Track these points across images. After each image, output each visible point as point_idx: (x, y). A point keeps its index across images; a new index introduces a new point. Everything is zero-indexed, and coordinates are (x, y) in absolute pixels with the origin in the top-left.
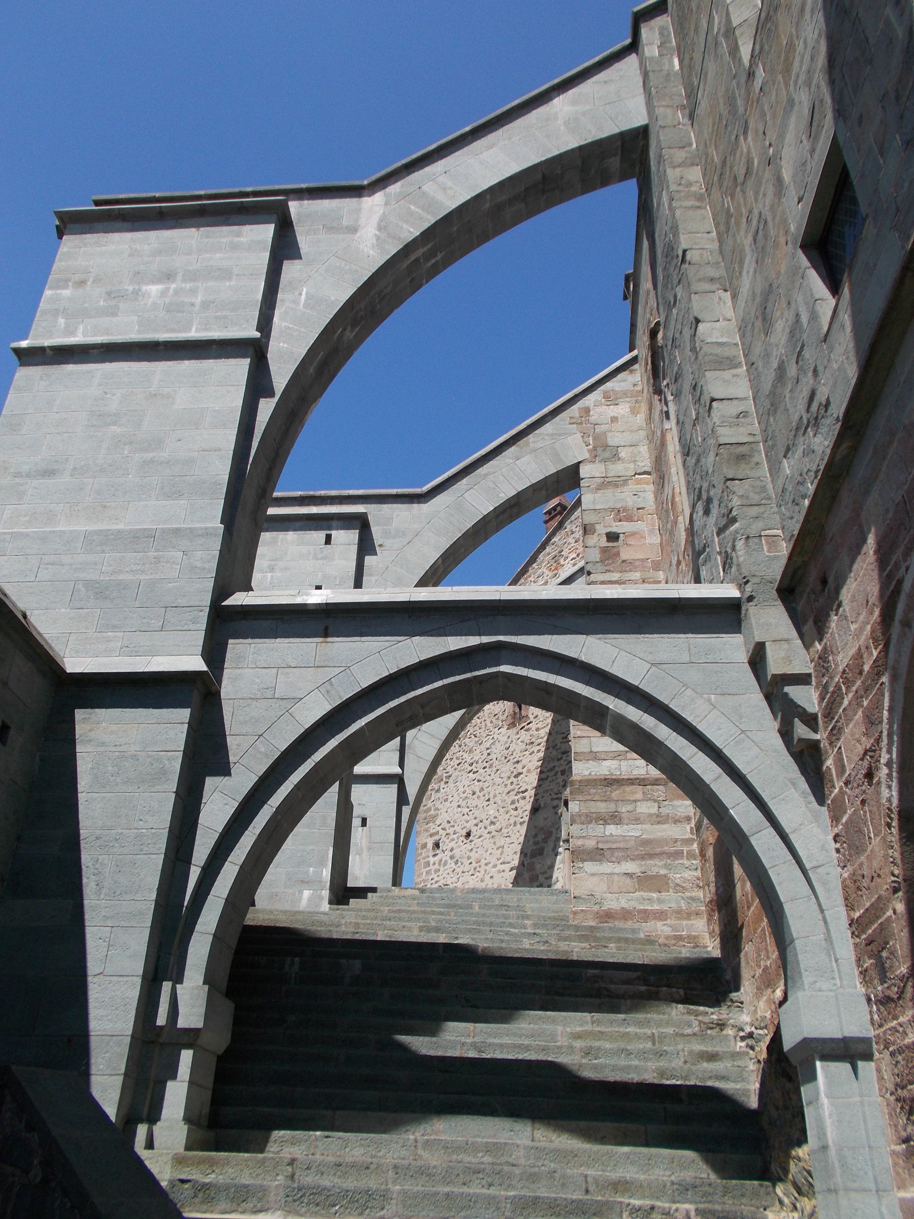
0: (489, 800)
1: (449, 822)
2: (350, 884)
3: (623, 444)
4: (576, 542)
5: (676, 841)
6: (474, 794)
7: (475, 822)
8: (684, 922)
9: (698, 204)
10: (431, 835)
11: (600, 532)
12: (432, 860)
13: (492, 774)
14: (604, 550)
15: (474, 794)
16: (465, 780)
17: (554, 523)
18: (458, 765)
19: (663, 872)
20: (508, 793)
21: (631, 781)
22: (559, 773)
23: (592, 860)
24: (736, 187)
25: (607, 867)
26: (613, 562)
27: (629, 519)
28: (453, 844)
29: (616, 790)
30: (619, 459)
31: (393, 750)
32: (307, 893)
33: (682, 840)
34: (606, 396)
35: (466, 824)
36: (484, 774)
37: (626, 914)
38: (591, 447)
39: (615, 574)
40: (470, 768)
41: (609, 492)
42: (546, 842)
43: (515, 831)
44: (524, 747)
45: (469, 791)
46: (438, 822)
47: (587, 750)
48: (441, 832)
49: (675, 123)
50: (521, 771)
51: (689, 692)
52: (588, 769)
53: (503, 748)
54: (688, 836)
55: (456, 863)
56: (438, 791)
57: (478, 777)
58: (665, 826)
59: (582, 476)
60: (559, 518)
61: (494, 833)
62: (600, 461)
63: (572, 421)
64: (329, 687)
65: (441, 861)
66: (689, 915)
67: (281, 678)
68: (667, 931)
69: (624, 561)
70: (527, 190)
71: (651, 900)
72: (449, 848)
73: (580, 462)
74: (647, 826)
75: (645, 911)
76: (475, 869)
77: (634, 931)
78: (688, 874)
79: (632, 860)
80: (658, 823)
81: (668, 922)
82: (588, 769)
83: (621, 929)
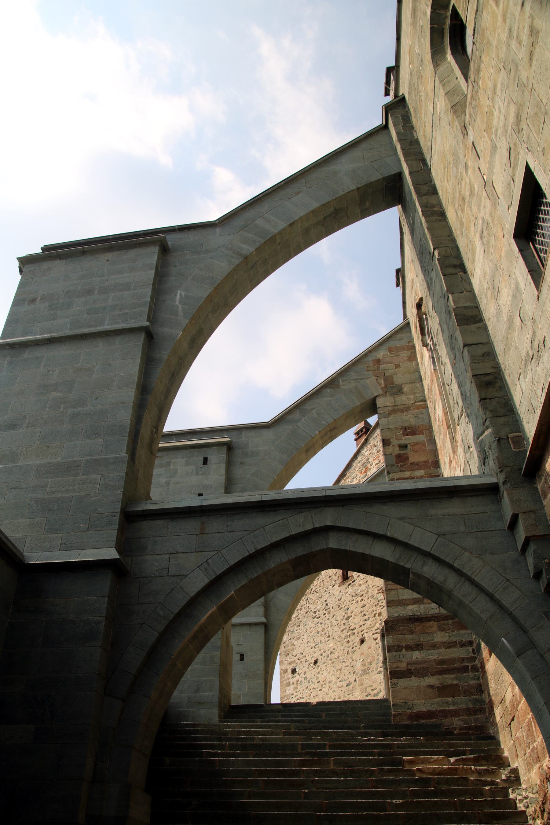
0: (329, 637)
2: (233, 703)
3: (405, 382)
4: (378, 452)
5: (463, 660)
6: (318, 633)
7: (320, 652)
8: (472, 717)
9: (440, 218)
10: (290, 664)
11: (394, 444)
12: (291, 681)
13: (330, 618)
14: (399, 456)
15: (318, 633)
16: (311, 624)
17: (363, 440)
19: (455, 682)
20: (342, 631)
21: (429, 619)
22: (377, 615)
24: (465, 204)
25: (414, 682)
26: (405, 464)
27: (414, 433)
28: (306, 669)
29: (418, 626)
30: (403, 393)
33: (468, 658)
34: (390, 350)
35: (314, 655)
36: (324, 619)
37: (430, 714)
38: (383, 385)
39: (406, 473)
40: (314, 615)
41: (397, 416)
42: (371, 664)
43: (349, 658)
44: (351, 598)
48: (297, 661)
49: (419, 169)
50: (350, 615)
52: (397, 612)
54: (471, 655)
55: (309, 682)
58: (455, 649)
59: (378, 406)
61: (334, 660)
62: (390, 395)
64: (206, 566)
65: (298, 681)
66: (475, 712)
68: (460, 724)
70: (325, 218)
72: (303, 672)
73: (375, 397)
76: (322, 686)
77: (438, 726)
78: (473, 682)
79: (432, 675)
80: (450, 648)
81: (461, 717)
82: (397, 612)
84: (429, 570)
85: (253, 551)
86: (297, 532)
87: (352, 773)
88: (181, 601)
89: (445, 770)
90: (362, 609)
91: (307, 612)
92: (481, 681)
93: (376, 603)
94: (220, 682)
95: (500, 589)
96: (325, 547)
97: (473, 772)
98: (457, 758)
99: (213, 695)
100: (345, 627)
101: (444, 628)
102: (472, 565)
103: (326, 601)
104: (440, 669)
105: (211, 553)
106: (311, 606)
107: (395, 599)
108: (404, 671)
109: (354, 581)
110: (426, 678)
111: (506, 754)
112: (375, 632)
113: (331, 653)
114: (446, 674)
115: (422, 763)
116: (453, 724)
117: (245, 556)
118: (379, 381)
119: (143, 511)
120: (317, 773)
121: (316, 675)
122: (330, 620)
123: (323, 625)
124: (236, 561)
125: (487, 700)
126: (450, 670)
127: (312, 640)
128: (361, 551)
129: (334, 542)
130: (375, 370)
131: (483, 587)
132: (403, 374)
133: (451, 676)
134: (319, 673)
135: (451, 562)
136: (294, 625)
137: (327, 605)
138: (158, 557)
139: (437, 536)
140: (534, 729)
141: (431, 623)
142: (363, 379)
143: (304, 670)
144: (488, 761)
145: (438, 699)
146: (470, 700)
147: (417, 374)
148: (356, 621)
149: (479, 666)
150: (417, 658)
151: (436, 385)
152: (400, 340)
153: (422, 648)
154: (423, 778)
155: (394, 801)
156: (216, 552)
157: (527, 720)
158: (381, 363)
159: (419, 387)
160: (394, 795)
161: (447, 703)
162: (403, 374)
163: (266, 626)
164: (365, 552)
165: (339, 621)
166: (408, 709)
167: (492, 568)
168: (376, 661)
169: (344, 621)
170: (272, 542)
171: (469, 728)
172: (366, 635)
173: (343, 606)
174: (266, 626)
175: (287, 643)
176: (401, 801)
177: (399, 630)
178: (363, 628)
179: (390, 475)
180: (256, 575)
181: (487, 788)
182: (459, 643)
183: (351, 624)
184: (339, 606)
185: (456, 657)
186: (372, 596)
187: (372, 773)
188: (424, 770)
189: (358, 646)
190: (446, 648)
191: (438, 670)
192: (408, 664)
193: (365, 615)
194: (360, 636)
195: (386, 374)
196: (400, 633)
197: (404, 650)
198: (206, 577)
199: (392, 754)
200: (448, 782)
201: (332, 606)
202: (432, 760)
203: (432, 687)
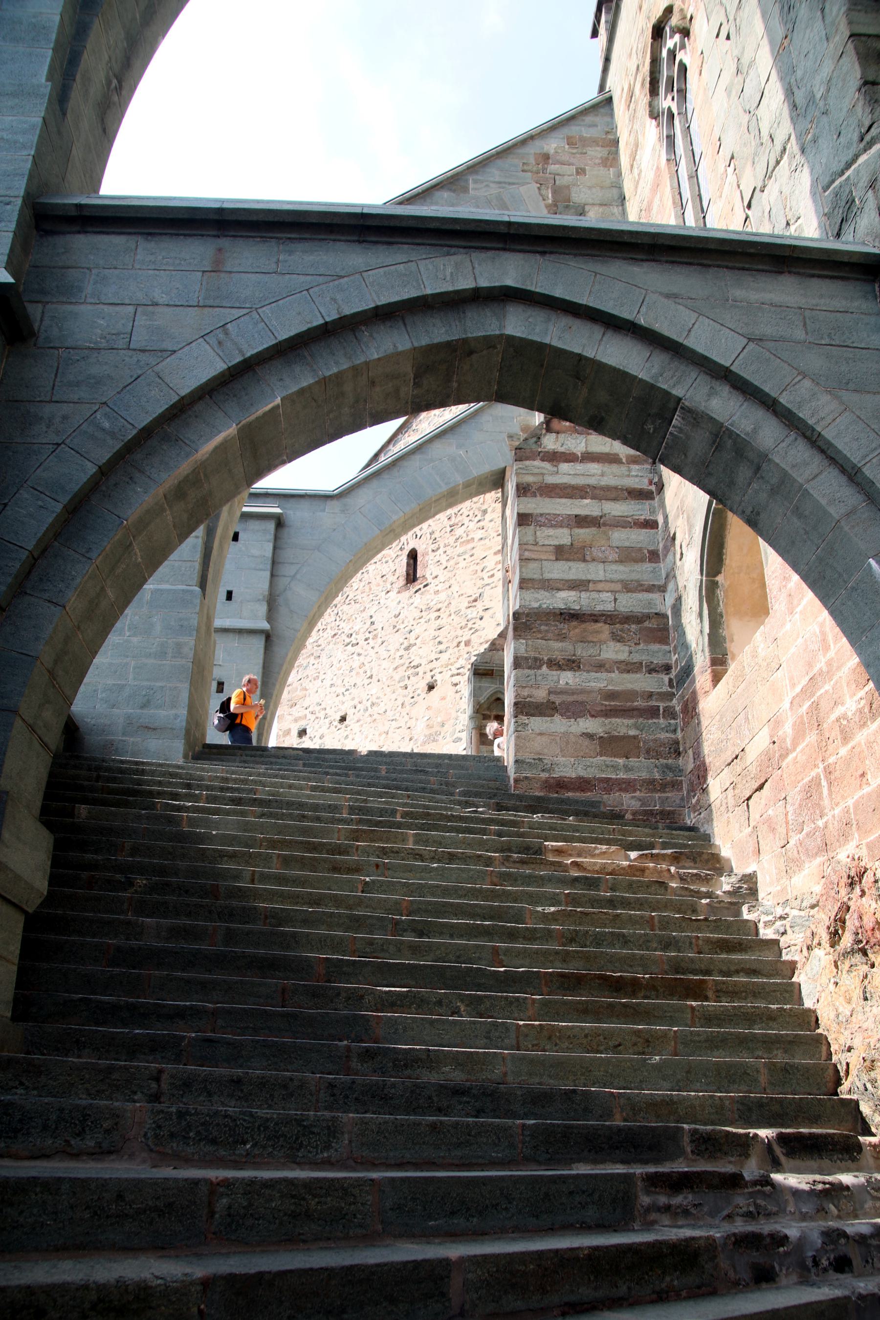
0: (371, 677)
2: (208, 742)
3: (591, 201)
5: (650, 695)
7: (353, 703)
10: (296, 720)
13: (377, 646)
19: (632, 732)
20: (396, 668)
21: (595, 617)
22: (463, 644)
23: (542, 714)
25: (558, 724)
28: (324, 730)
29: (575, 627)
31: (259, 600)
33: (659, 694)
34: (571, 142)
35: (340, 706)
36: (366, 647)
37: (583, 784)
38: (550, 201)
40: (348, 640)
43: (404, 714)
44: (417, 614)
50: (412, 641)
51: (807, 383)
54: (666, 688)
58: (638, 675)
63: (525, 168)
64: (221, 336)
66: (664, 786)
67: (141, 320)
68: (635, 805)
71: (616, 767)
74: (615, 675)
75: (608, 780)
77: (593, 804)
78: (663, 736)
79: (592, 716)
80: (628, 672)
81: (638, 794)
83: (577, 802)
84: (724, 406)
85: (334, 316)
86: (438, 291)
87: (452, 858)
88: (153, 404)
89: (623, 869)
90: (437, 633)
91: (335, 635)
92: (679, 735)
93: (463, 624)
94: (190, 693)
95: (874, 461)
96: (497, 332)
97: (672, 876)
98: (641, 853)
99: (176, 717)
100: (402, 661)
101: (622, 638)
102: (818, 408)
103: (371, 617)
104: (608, 708)
105: (234, 311)
106: (342, 625)
107: (535, 576)
108: (542, 704)
109: (425, 586)
110: (581, 721)
111: (726, 851)
112: (456, 672)
113: (373, 704)
115: (579, 856)
116: (622, 804)
117: (315, 324)
118: (543, 192)
119: (79, 206)
120: (384, 852)
121: (342, 740)
122: (376, 650)
123: (362, 658)
124: (292, 334)
125: (690, 766)
126: (624, 711)
127: (339, 682)
128: (577, 350)
129: (517, 324)
130: (538, 173)
131: (839, 452)
132: (590, 188)
133: (626, 721)
134: (347, 737)
135: (774, 394)
137: (372, 623)
138: (106, 308)
139: (745, 341)
140: (825, 791)
142: (514, 184)
143: (320, 732)
144: (695, 863)
145: (599, 758)
147: (615, 191)
148: (422, 653)
149: (678, 709)
150: (567, 684)
151: (668, 189)
152: (590, 126)
153: (579, 667)
154: (586, 878)
155: (539, 909)
156: (247, 311)
157: (806, 780)
158: (551, 162)
159: (617, 214)
160: (535, 899)
161: (615, 768)
162: (590, 188)
163: (268, 637)
164: (585, 354)
165: (392, 652)
166: (543, 770)
167: (858, 417)
168: (452, 721)
169: (402, 652)
170: (379, 304)
171: (651, 813)
172: (438, 677)
173: (402, 626)
174: (268, 637)
175: (294, 685)
176: (552, 909)
177: (540, 632)
178: (435, 664)
180: (335, 370)
181: (703, 901)
182: (647, 666)
184: (395, 627)
185: (637, 689)
186: (458, 612)
187: (489, 862)
188: (585, 865)
189: (423, 695)
191: (604, 708)
192: (550, 693)
193: (440, 643)
194: (428, 679)
195: (557, 183)
196: (540, 636)
197: (544, 667)
199: (522, 835)
200: (630, 887)
202: (597, 852)
203: (590, 736)
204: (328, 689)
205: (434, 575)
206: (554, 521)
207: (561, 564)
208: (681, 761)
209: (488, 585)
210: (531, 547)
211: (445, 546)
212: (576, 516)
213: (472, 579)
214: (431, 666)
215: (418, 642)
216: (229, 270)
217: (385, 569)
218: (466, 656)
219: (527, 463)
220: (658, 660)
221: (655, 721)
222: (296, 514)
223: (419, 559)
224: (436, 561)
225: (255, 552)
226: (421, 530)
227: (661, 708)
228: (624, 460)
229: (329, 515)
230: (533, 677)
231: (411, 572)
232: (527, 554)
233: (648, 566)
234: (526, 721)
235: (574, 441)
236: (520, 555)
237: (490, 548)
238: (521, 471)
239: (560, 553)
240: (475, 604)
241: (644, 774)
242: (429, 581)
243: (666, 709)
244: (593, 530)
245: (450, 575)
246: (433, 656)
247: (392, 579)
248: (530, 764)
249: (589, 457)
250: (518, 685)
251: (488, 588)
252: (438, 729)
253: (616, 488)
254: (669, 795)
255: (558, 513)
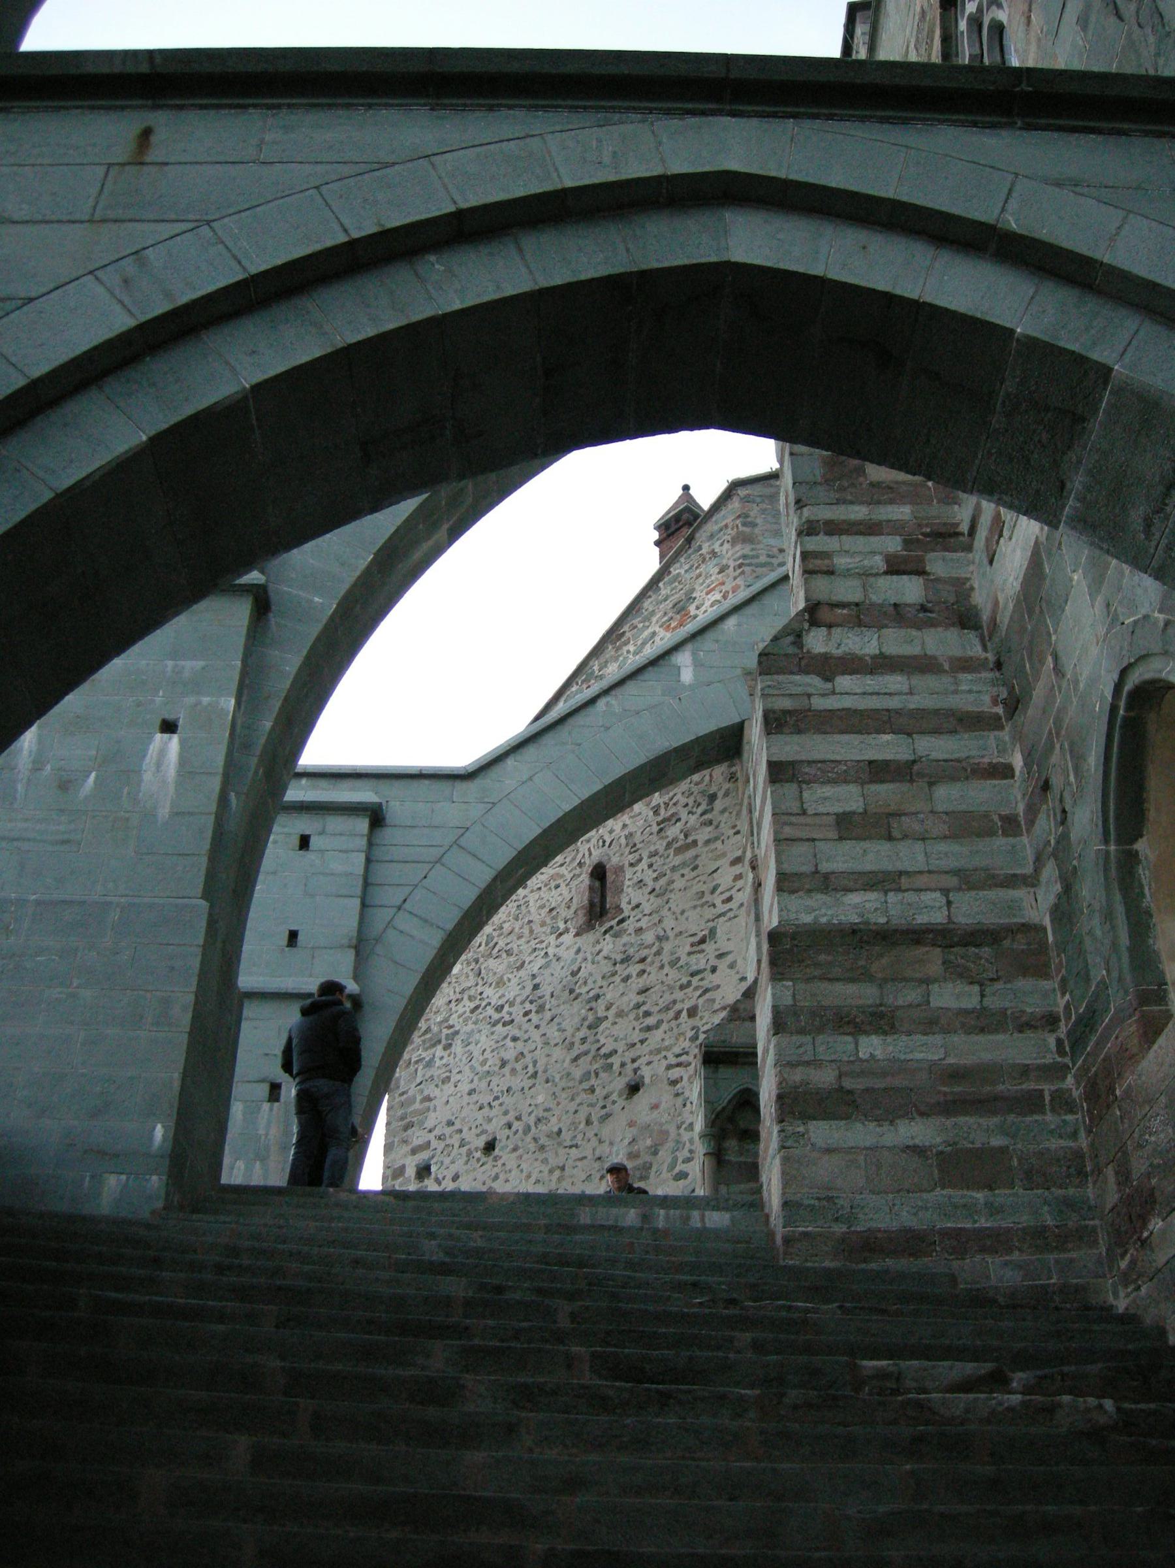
0: (535, 1075)
1: (450, 1123)
5: (1025, 1071)
6: (504, 1063)
7: (504, 1120)
8: (1052, 1257)
10: (414, 1152)
13: (543, 1024)
16: (485, 1040)
18: (472, 1011)
19: (997, 1141)
20: (576, 1059)
21: (917, 936)
22: (684, 1013)
25: (860, 1134)
28: (459, 1166)
29: (882, 955)
31: (342, 947)
32: (113, 1182)
35: (486, 1127)
36: (525, 1026)
37: (913, 1242)
39: (856, 508)
40: (496, 1016)
42: (655, 1153)
43: (590, 1134)
44: (607, 968)
45: (493, 1062)
46: (429, 1124)
47: (807, 869)
48: (434, 1143)
50: (601, 1014)
53: (566, 972)
54: (1051, 1058)
56: (430, 1064)
57: (512, 1030)
60: (686, 532)
66: (1063, 1239)
69: (872, 485)
72: (449, 1174)
74: (957, 1039)
78: (1054, 1144)
79: (922, 1114)
80: (982, 1030)
81: (1016, 1256)
89: (1011, 1409)
90: (641, 999)
91: (477, 1008)
93: (684, 980)
98: (1039, 1373)
100: (585, 1047)
104: (949, 1098)
105: (161, 227)
106: (489, 991)
112: (673, 1060)
114: (966, 1114)
116: (988, 1277)
123: (520, 1044)
127: (484, 1084)
128: (881, 286)
129: (753, 241)
133: (984, 1121)
134: (496, 1177)
136: (434, 1045)
141: (921, 951)
143: (454, 1169)
146: (1046, 1202)
153: (893, 1027)
161: (970, 1209)
166: (837, 1220)
170: (464, 205)
172: (646, 1072)
173: (584, 990)
175: (410, 1093)
177: (817, 965)
178: (639, 1050)
179: (805, 510)
183: (603, 1041)
184: (571, 991)
186: (673, 964)
189: (621, 1102)
190: (968, 1033)
193: (647, 1014)
198: (118, 308)
201: (549, 990)
204: (466, 1098)
205: (634, 903)
206: (833, 773)
207: (847, 845)
208: (1090, 1192)
209: (723, 914)
210: (793, 819)
211: (652, 855)
212: (870, 762)
213: (695, 907)
214: (632, 1054)
215: (611, 1013)
216: (160, 160)
217: (554, 898)
218: (690, 1034)
219: (781, 678)
220: (1033, 1006)
221: (1036, 1117)
222: (400, 805)
223: (610, 877)
224: (635, 880)
225: (336, 865)
226: (611, 832)
227: (1047, 1098)
228: (947, 667)
229: (455, 808)
230: (810, 1047)
231: (597, 900)
232: (788, 831)
233: (1000, 842)
234: (801, 1129)
235: (857, 639)
236: (776, 833)
237: (724, 855)
238: (771, 691)
239: (847, 826)
240: (703, 946)
241: (1025, 1218)
242: (626, 914)
243: (1055, 1095)
244: (905, 787)
245: (659, 901)
246: (636, 1036)
247: (564, 913)
248: (812, 1208)
249: (883, 664)
250: (784, 1064)
251: (722, 919)
252: (648, 1158)
253: (936, 712)
254: (1074, 1255)
255: (838, 758)
